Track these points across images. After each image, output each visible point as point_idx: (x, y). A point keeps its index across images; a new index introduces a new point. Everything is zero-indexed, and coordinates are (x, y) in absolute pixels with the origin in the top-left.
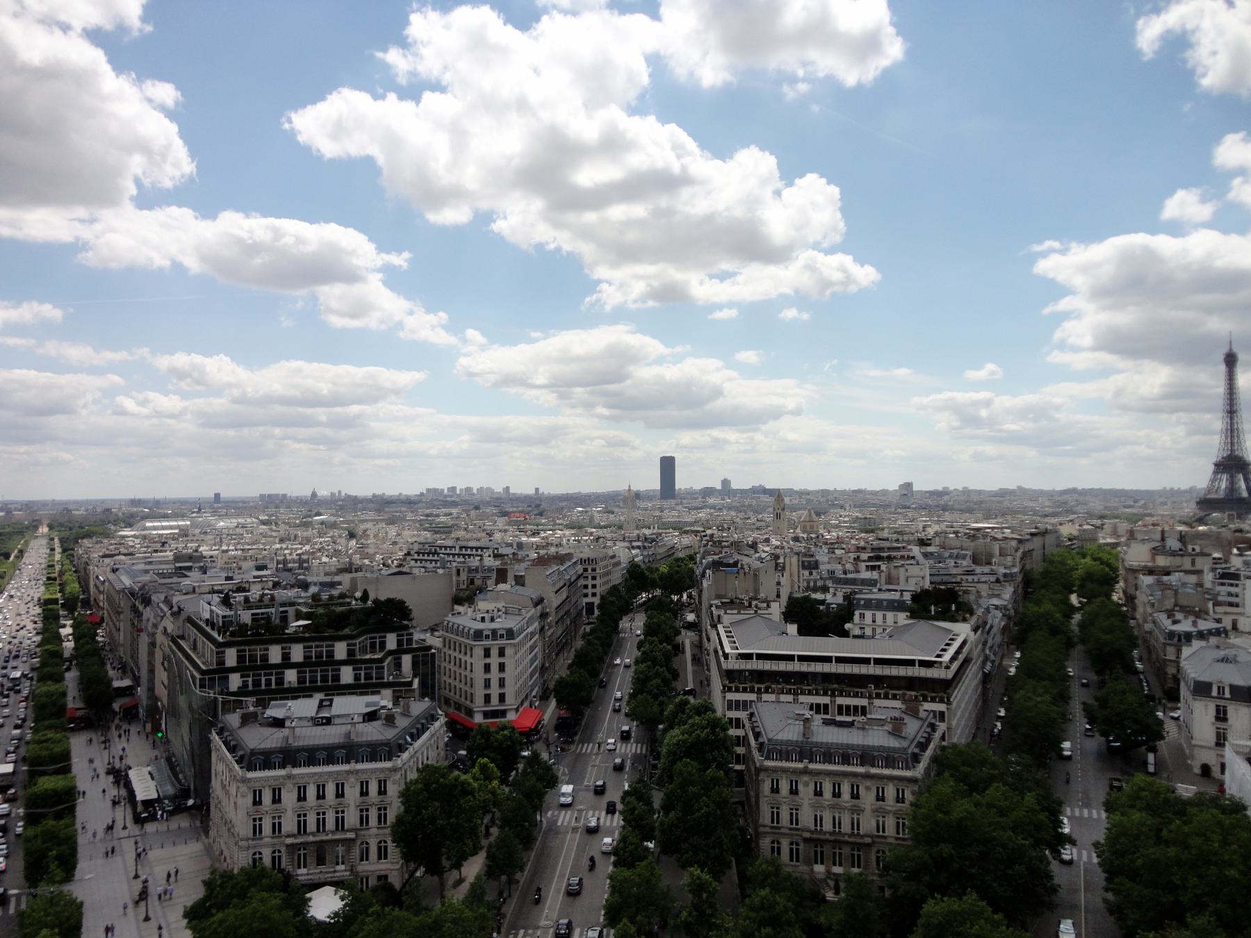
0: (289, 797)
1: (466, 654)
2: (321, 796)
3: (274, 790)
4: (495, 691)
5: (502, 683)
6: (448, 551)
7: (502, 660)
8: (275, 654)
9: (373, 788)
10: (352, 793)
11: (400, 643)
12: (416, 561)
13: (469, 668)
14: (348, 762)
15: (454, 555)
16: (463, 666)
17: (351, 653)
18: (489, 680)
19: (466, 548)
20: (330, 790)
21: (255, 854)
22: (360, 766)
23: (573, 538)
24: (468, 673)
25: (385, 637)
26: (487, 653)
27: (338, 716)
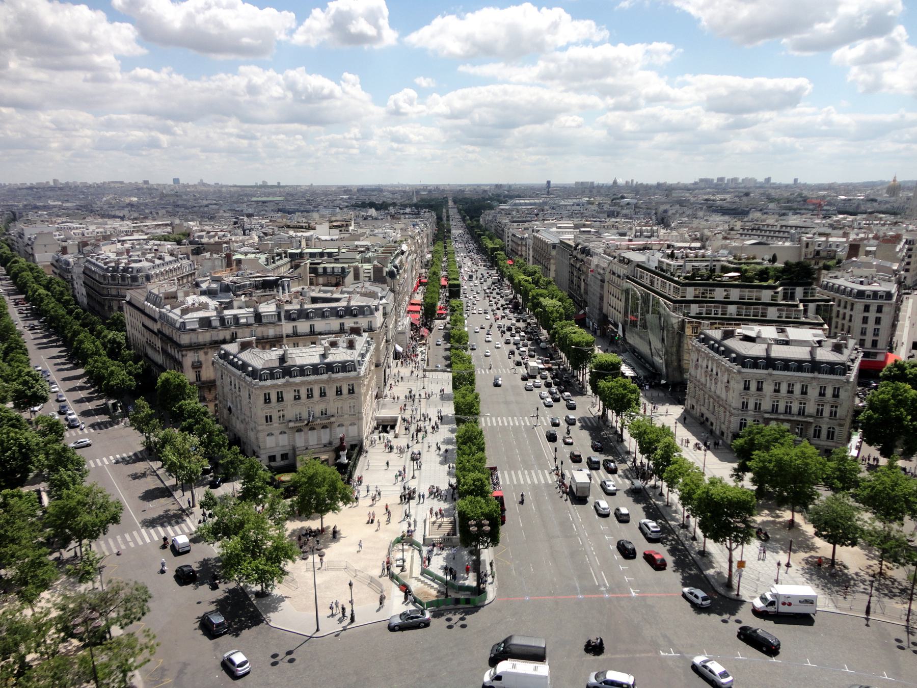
0: (768, 388)
1: (845, 307)
2: (790, 392)
3: (758, 382)
4: (869, 338)
5: (876, 332)
6: (770, 228)
7: (879, 315)
8: (719, 294)
9: (829, 392)
10: (813, 393)
11: (805, 294)
12: (741, 234)
13: (847, 318)
14: (812, 372)
15: (775, 232)
16: (841, 316)
17: (774, 298)
18: (866, 328)
19: (786, 226)
20: (797, 389)
21: (742, 420)
22: (821, 376)
23: (864, 222)
24: (846, 322)
25: (794, 289)
26: (867, 308)
27: (795, 341)
